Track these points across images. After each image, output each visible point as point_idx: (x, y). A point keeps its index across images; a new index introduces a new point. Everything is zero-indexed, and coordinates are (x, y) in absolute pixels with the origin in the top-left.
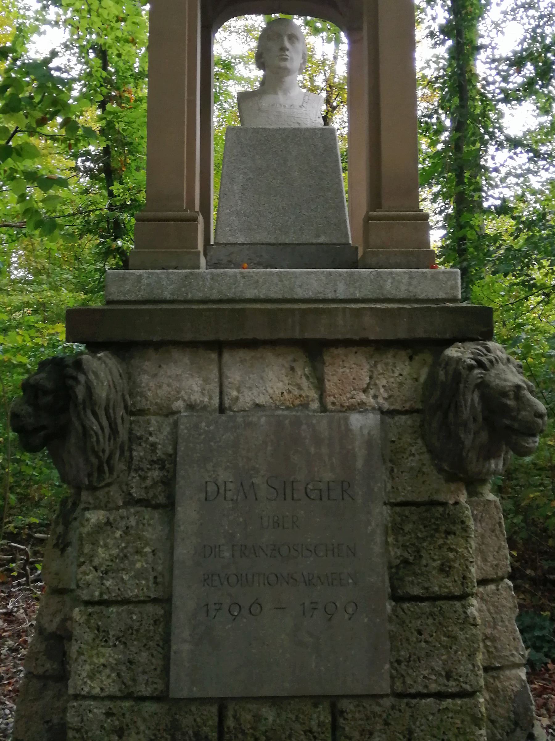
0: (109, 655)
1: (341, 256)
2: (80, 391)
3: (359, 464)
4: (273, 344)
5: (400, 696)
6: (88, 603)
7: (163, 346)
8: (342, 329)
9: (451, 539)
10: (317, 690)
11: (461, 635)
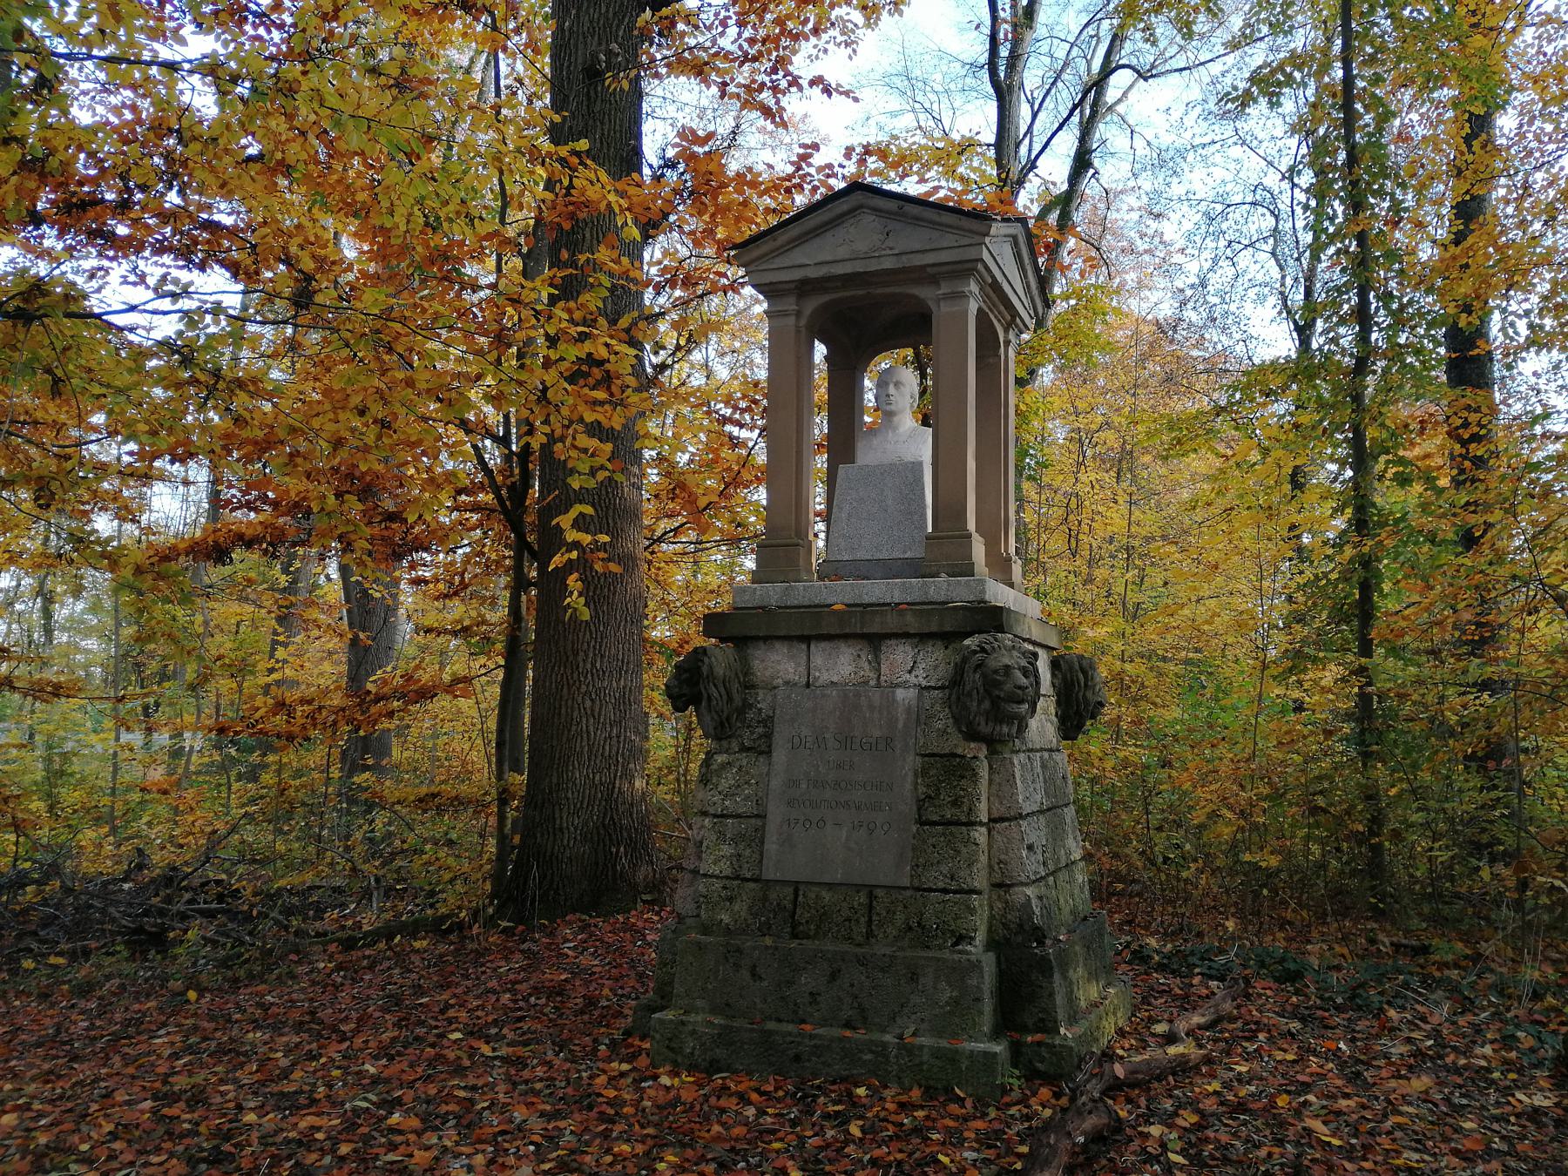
0: (726, 850)
1: (917, 569)
2: (705, 669)
3: (900, 725)
4: (845, 637)
5: (918, 889)
6: (715, 816)
7: (766, 639)
8: (892, 623)
9: (963, 782)
11: (964, 850)
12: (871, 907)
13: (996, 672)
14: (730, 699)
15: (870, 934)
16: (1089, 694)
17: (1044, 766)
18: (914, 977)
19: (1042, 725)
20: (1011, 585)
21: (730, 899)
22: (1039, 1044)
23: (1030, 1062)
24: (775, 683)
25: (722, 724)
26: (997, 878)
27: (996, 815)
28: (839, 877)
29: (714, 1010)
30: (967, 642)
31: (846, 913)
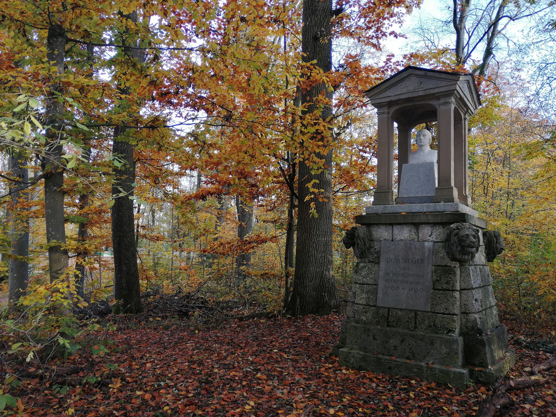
0: (364, 295)
2: (356, 234)
3: (426, 255)
4: (406, 224)
5: (433, 313)
6: (360, 284)
7: (378, 224)
8: (423, 219)
9: (450, 275)
10: (412, 309)
12: (416, 318)
13: (463, 236)
14: (365, 245)
15: (416, 327)
16: (498, 245)
17: (481, 271)
18: (432, 343)
19: (480, 257)
20: (467, 206)
21: (366, 312)
22: (480, 371)
23: (477, 377)
24: (381, 239)
25: (362, 253)
26: (463, 310)
27: (463, 287)
28: (404, 307)
29: (360, 349)
30: (451, 226)
31: (407, 319)
